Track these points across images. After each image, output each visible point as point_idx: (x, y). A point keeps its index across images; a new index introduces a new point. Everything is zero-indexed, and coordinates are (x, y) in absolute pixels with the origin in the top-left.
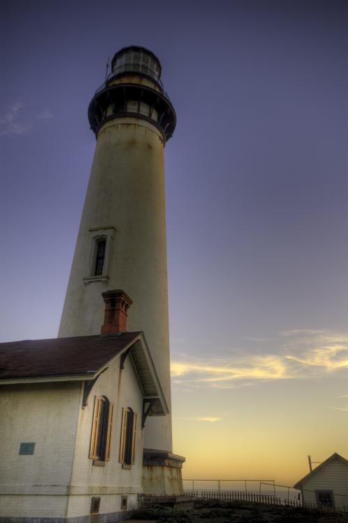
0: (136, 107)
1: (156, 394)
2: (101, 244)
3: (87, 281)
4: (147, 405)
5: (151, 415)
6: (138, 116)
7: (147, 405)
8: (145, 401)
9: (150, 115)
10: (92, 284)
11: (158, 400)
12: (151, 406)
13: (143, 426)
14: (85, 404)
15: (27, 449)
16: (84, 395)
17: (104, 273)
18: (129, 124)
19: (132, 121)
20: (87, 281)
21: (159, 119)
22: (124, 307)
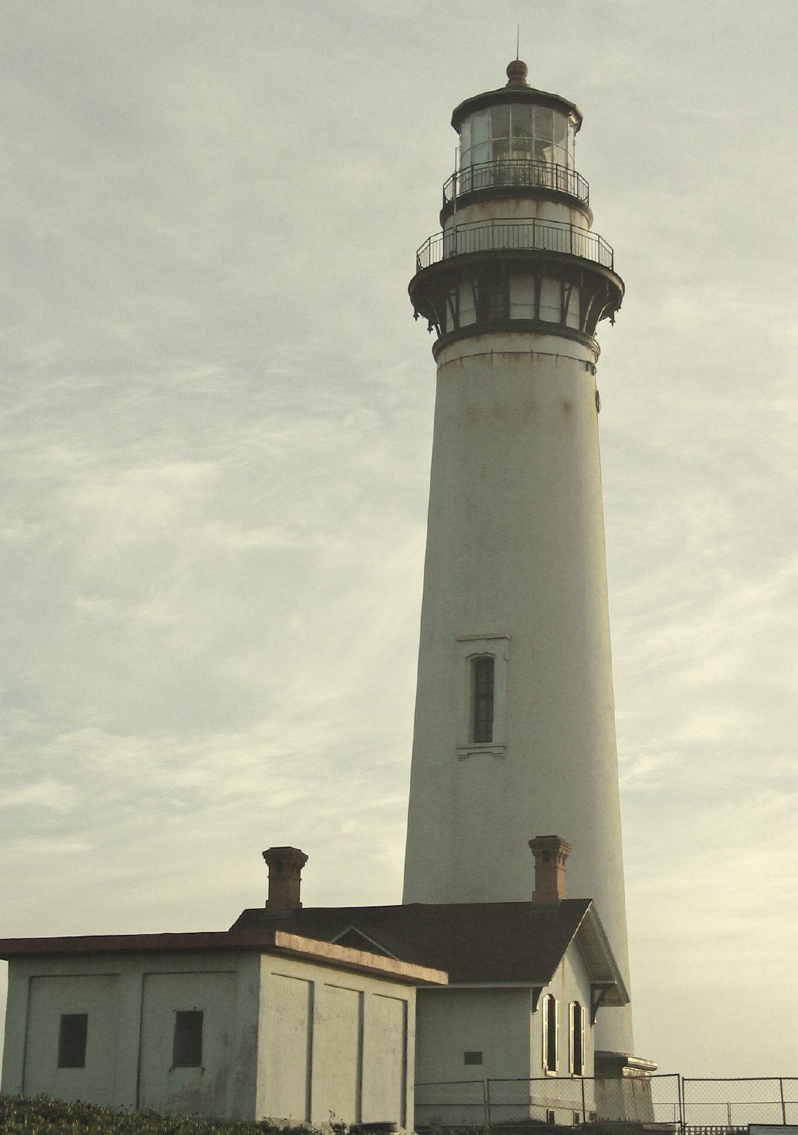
0: (529, 297)
1: (611, 978)
2: (483, 668)
3: (465, 752)
4: (598, 993)
5: (602, 1006)
6: (536, 327)
7: (598, 993)
8: (593, 987)
9: (564, 312)
10: (471, 757)
11: (614, 984)
12: (603, 994)
13: (592, 1022)
14: (535, 1010)
15: (473, 1058)
16: (533, 1001)
17: (497, 736)
18: (517, 355)
19: (522, 343)
20: (465, 752)
21: (581, 325)
22: (561, 859)
